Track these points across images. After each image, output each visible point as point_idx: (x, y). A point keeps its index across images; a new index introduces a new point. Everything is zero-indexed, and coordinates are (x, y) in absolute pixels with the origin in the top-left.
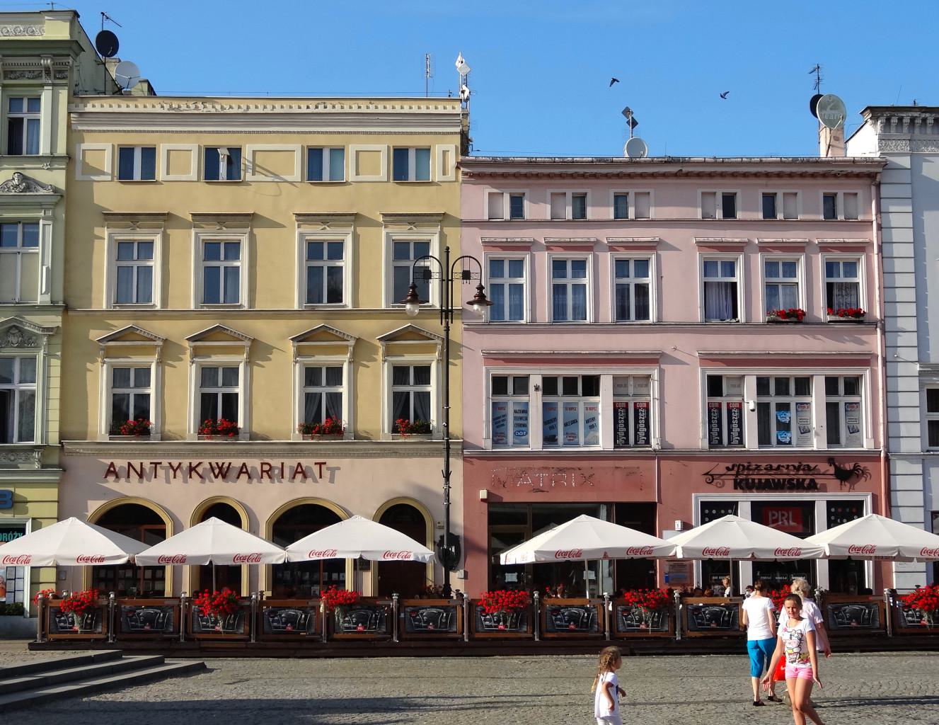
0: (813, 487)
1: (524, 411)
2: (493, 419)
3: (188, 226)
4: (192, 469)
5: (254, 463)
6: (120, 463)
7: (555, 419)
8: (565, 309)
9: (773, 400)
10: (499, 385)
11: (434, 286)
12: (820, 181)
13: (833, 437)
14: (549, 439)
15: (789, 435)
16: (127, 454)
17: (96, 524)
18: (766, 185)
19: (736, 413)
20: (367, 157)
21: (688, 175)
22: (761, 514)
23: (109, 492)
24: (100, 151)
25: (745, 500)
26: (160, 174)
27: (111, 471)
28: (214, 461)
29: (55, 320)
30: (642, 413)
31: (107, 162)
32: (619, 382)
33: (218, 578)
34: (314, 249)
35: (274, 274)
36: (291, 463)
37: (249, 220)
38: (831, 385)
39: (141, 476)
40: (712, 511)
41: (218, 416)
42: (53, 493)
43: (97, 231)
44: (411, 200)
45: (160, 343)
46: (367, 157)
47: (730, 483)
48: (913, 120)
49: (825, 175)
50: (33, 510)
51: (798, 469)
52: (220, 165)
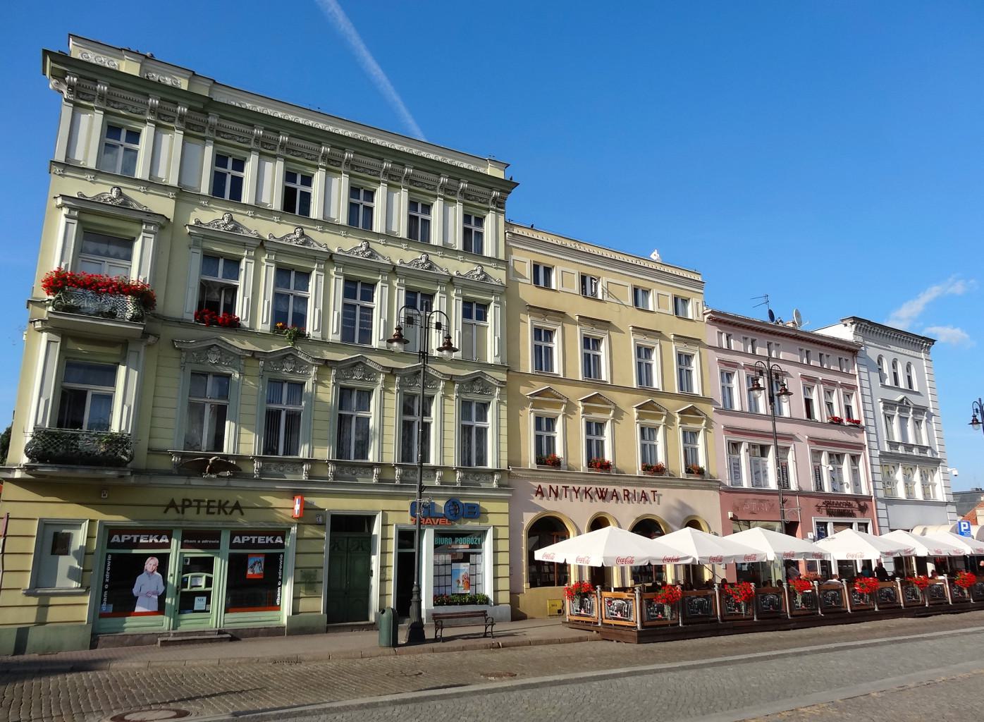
3: (574, 323)
4: (586, 492)
5: (620, 490)
6: (545, 486)
17: (590, 531)
23: (535, 508)
24: (523, 261)
27: (540, 492)
28: (598, 487)
29: (502, 376)
31: (528, 272)
39: (556, 495)
42: (504, 507)
43: (522, 316)
45: (565, 401)
50: (493, 520)
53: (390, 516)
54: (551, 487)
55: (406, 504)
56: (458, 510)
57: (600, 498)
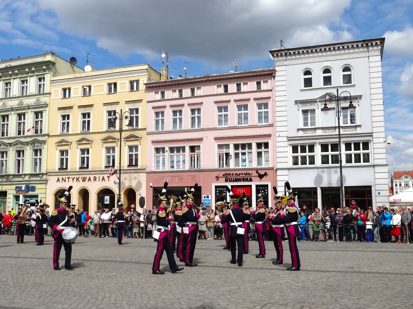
0: (251, 180)
2: (157, 161)
6: (60, 178)
7: (174, 161)
9: (240, 151)
11: (118, 122)
12: (254, 78)
13: (259, 163)
15: (245, 163)
18: (238, 81)
20: (123, 85)
21: (210, 81)
26: (72, 95)
34: (109, 113)
35: (99, 121)
36: (101, 176)
37: (91, 106)
38: (259, 145)
41: (84, 164)
44: (134, 96)
46: (123, 85)
47: (224, 179)
48: (286, 54)
49: (257, 76)
51: (246, 174)
52: (87, 91)
54: (63, 179)
55: (14, 187)
56: (28, 188)
57: (83, 181)
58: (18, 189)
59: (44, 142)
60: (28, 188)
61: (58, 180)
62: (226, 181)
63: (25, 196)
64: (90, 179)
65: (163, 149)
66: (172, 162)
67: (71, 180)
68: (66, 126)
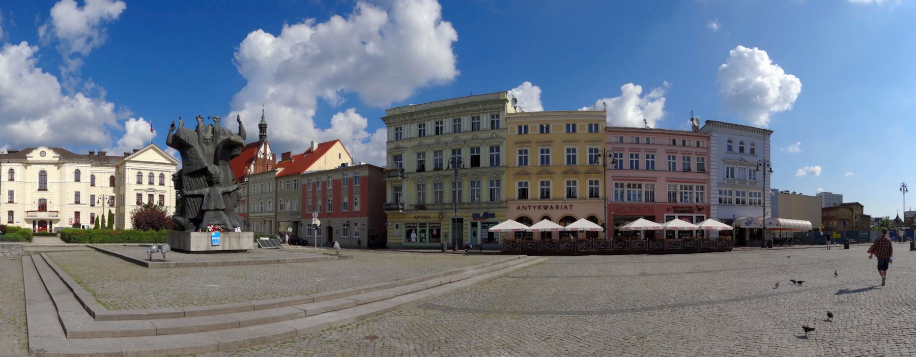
1: (622, 193)
8: (635, 166)
9: (684, 191)
10: (617, 185)
14: (629, 199)
16: (523, 203)
19: (675, 194)
22: (680, 218)
25: (677, 215)
30: (652, 193)
32: (647, 185)
33: (546, 235)
35: (558, 157)
40: (670, 218)
41: (545, 195)
53: (467, 217)
55: (471, 214)
56: (487, 215)
58: (476, 216)
59: (503, 172)
60: (487, 215)
61: (519, 208)
62: (675, 212)
63: (483, 223)
64: (552, 207)
65: (622, 186)
66: (629, 195)
67: (532, 208)
68: (523, 161)
